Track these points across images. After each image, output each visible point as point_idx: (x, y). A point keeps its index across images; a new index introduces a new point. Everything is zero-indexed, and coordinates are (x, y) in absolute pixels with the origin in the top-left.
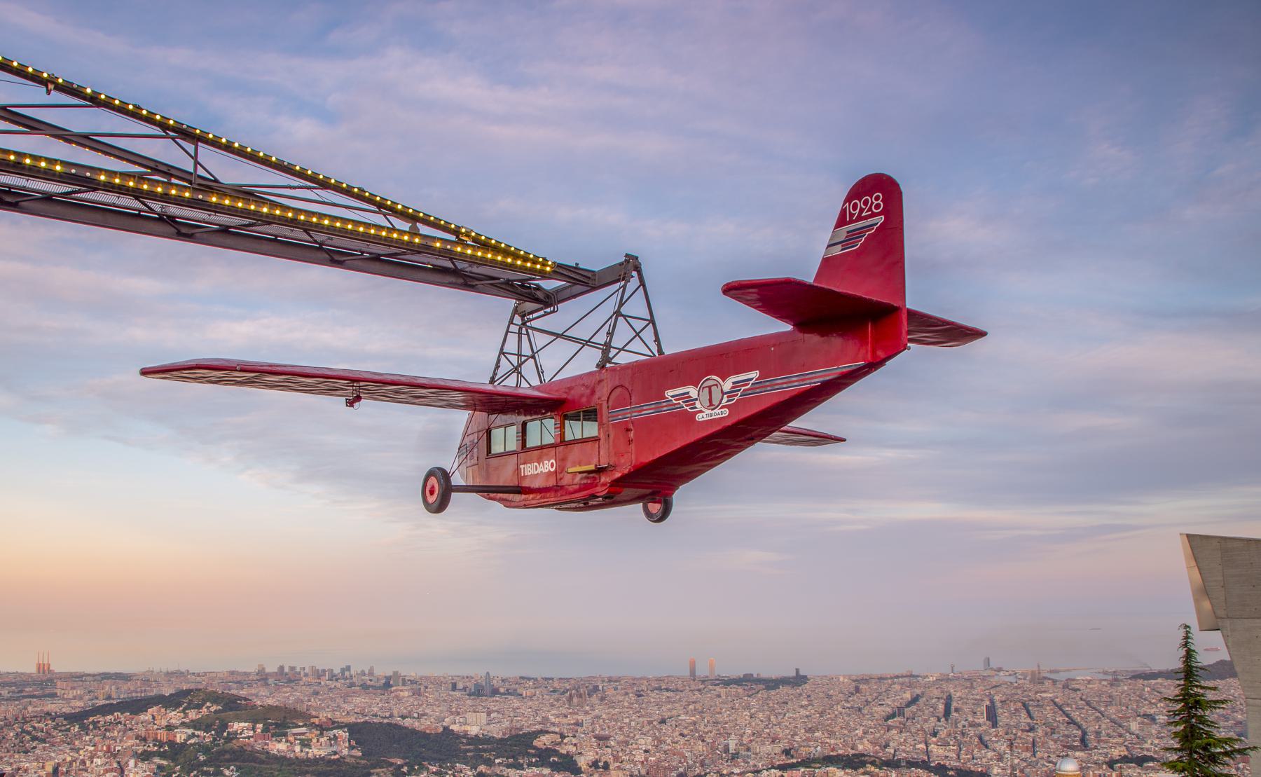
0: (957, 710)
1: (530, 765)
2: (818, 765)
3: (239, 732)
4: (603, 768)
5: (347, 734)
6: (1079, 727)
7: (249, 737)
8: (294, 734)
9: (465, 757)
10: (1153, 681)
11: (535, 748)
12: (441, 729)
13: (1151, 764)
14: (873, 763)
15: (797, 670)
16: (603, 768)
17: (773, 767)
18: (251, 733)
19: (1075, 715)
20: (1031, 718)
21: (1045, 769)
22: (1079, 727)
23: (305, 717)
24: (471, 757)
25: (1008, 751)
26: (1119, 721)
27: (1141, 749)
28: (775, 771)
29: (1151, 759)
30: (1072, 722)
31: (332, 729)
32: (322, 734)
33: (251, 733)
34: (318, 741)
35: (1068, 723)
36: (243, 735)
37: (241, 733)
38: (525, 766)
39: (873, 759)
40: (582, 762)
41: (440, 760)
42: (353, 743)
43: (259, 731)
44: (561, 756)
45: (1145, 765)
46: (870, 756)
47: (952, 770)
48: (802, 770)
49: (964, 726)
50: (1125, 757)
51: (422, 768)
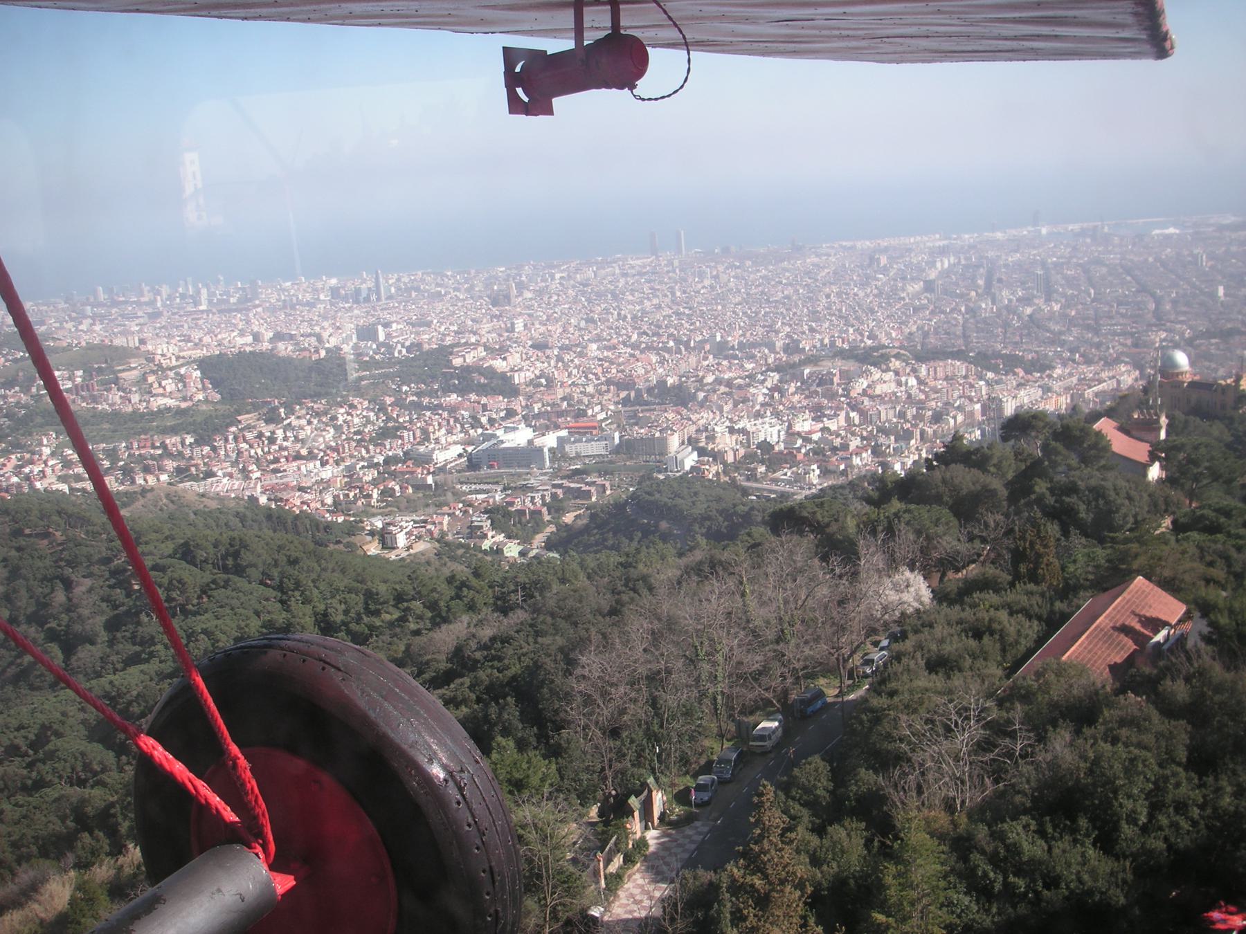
12: (323, 353)
22: (1153, 295)
43: (79, 380)
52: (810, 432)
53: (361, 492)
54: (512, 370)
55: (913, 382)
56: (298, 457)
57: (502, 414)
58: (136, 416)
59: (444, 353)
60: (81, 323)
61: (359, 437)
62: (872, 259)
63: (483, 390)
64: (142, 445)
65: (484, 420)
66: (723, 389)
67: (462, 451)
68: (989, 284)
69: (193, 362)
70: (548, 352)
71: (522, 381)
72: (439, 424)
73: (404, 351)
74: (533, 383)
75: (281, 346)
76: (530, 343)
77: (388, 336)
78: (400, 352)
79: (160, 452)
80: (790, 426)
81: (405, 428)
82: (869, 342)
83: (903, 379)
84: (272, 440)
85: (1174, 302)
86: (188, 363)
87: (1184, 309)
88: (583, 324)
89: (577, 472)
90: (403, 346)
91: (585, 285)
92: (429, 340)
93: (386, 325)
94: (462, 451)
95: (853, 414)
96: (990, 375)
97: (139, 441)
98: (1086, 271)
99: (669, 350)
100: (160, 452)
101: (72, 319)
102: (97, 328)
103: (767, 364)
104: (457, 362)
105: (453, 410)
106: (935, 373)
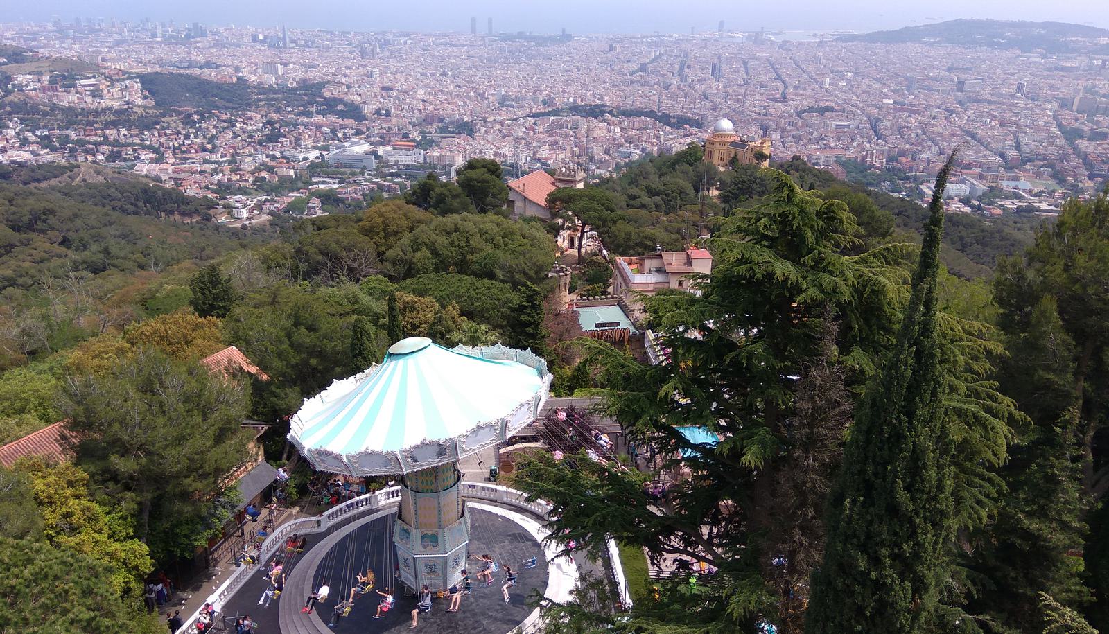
0: (689, 67)
1: (318, 113)
2: (566, 114)
3: (24, 84)
4: (385, 115)
5: (139, 85)
6: (784, 82)
7: (35, 90)
8: (83, 86)
9: (257, 106)
10: (850, 44)
11: (323, 97)
12: (235, 80)
13: (830, 113)
14: (611, 113)
15: (564, 31)
16: (385, 115)
17: (529, 116)
18: (38, 86)
19: (782, 71)
20: (747, 74)
22: (784, 82)
23: (95, 69)
24: (263, 106)
25: (723, 102)
26: (816, 77)
27: (827, 100)
29: (832, 109)
30: (779, 78)
31: (124, 80)
32: (112, 85)
33: (38, 86)
34: (109, 91)
35: (775, 79)
36: (29, 88)
37: (26, 86)
38: (315, 114)
39: (611, 109)
40: (367, 110)
41: (233, 108)
42: (146, 93)
44: (346, 104)
46: (609, 106)
47: (674, 118)
48: (552, 118)
49: (693, 81)
50: (812, 107)
51: (212, 115)
52: (547, 158)
53: (241, 177)
54: (364, 103)
55: (618, 130)
56: (204, 150)
57: (353, 132)
58: (85, 112)
59: (322, 85)
60: (63, 42)
62: (611, 46)
63: (342, 115)
64: (87, 133)
65: (340, 135)
66: (498, 126)
67: (318, 155)
68: (682, 69)
69: (137, 77)
70: (391, 93)
71: (370, 111)
72: (309, 136)
73: (295, 83)
74: (378, 112)
75: (206, 70)
76: (381, 85)
77: (286, 72)
78: (292, 84)
79: (102, 139)
80: (535, 153)
81: (285, 136)
82: (598, 102)
83: (612, 127)
84: (187, 137)
85: (797, 87)
86: (130, 78)
87: (802, 92)
88: (418, 76)
89: (392, 175)
90: (294, 80)
91: (425, 50)
92: (314, 76)
93: (286, 65)
94: (318, 155)
95: (575, 149)
97: (85, 130)
98: (745, 64)
99: (469, 98)
100: (102, 139)
101: (57, 38)
102: (76, 47)
103: (531, 112)
104: (327, 94)
105: (319, 127)
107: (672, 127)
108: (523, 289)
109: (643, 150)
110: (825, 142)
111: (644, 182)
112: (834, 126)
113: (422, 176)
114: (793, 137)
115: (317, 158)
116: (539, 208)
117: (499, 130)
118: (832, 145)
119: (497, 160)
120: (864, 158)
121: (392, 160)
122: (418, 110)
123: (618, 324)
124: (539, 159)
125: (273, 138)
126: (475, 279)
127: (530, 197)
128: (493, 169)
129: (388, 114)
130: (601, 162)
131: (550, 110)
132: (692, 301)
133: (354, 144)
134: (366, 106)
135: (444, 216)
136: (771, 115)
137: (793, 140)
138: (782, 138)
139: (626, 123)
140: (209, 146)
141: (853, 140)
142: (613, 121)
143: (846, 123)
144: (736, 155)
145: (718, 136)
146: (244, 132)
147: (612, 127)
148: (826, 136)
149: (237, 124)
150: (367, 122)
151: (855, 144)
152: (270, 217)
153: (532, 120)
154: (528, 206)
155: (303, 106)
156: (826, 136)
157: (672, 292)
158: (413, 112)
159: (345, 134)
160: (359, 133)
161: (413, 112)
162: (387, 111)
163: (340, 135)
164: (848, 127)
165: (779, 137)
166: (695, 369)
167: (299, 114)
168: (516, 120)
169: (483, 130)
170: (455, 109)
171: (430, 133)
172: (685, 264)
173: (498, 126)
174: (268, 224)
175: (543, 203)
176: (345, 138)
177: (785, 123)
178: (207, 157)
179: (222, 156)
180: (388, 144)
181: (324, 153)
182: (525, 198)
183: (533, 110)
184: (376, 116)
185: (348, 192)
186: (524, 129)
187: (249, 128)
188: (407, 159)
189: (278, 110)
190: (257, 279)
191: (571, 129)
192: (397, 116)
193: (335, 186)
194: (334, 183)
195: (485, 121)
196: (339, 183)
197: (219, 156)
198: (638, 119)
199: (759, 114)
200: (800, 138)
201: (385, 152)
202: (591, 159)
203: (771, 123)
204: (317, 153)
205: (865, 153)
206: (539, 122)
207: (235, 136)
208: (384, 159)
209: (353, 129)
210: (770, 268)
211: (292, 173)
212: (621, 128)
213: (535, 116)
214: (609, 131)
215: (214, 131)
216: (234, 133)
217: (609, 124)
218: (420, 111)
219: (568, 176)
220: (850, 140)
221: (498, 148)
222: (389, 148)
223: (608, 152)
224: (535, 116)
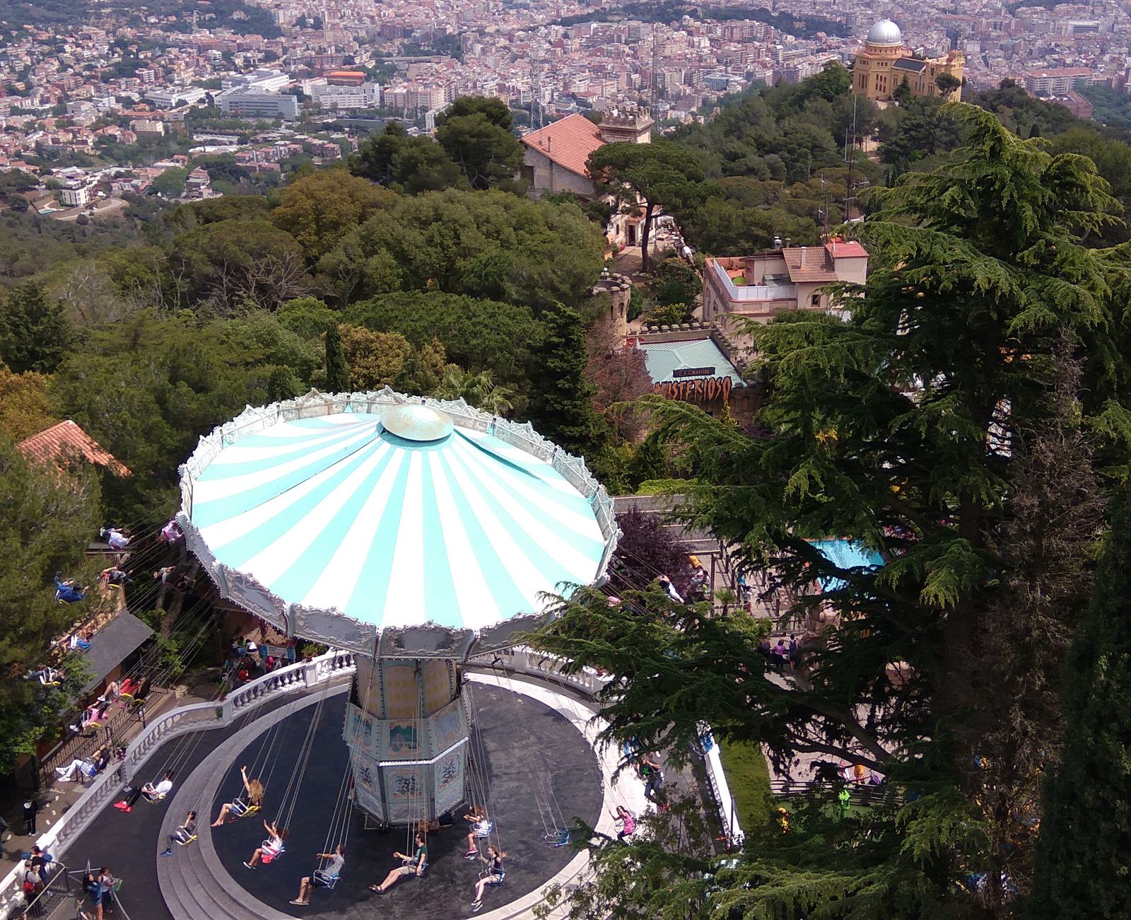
1: (202, 25)
2: (617, 18)
4: (313, 27)
9: (99, 16)
14: (693, 14)
16: (313, 27)
17: (555, 23)
21: (926, 16)
24: (109, 16)
28: (557, 28)
38: (195, 28)
40: (282, 18)
41: (59, 21)
45: (1058, 7)
47: (800, 20)
48: (594, 25)
51: (24, 33)
52: (588, 94)
53: (75, 137)
54: (277, 6)
55: (705, 43)
56: (13, 92)
57: (260, 56)
61: (88, 73)
65: (239, 62)
66: (503, 42)
67: (203, 96)
71: (287, 20)
72: (187, 64)
74: (301, 22)
80: (566, 86)
81: (146, 66)
83: (696, 39)
89: (327, 127)
94: (203, 96)
95: (634, 76)
96: (791, 38)
103: (558, 15)
105: (203, 49)
106: (732, 34)
107: (797, 36)
108: (551, 315)
109: (749, 75)
110: (1056, 56)
111: (750, 131)
112: (1070, 29)
113: (377, 128)
114: (1001, 48)
115: (201, 101)
116: (575, 179)
117: (505, 48)
118: (1069, 61)
119: (503, 99)
120: (1122, 81)
121: (326, 102)
122: (367, 16)
123: (712, 371)
124: (573, 96)
125: (127, 70)
126: (470, 301)
127: (561, 160)
128: (496, 113)
129: (318, 25)
130: (678, 97)
131: (591, 11)
132: (835, 329)
133: (262, 76)
134: (281, 12)
135: (415, 195)
136: (965, 13)
137: (1001, 53)
138: (983, 50)
139: (719, 32)
140: (20, 86)
141: (1103, 52)
142: (698, 29)
143: (1091, 23)
144: (905, 81)
145: (875, 49)
146: (78, 61)
147: (696, 39)
148: (1057, 46)
149: (67, 47)
150: (283, 39)
151: (1107, 58)
152: (125, 203)
153: (561, 29)
154: (556, 175)
155: (176, 14)
156: (1057, 46)
157: (802, 315)
158: (360, 20)
159: (246, 60)
160: (269, 57)
161: (360, 20)
162: (316, 19)
163: (239, 62)
164: (1095, 28)
165: (977, 49)
166: (842, 445)
167: (170, 28)
168: (533, 29)
169: (478, 47)
170: (431, 14)
171: (389, 55)
172: (822, 267)
173: (503, 42)
174: (121, 214)
175: (581, 169)
176: (246, 67)
177: (988, 25)
178: (17, 104)
179: (42, 102)
180: (320, 75)
181: (213, 94)
182: (552, 162)
183: (563, 13)
184: (298, 28)
185: (255, 157)
186: (547, 46)
187: (86, 53)
188: (352, 99)
189: (134, 22)
190: (105, 307)
191: (627, 43)
192: (334, 26)
193: (233, 149)
194: (231, 143)
195: (482, 33)
196: (240, 142)
197: (37, 101)
198: (739, 23)
199: (944, 11)
200: (1014, 49)
201: (315, 88)
202: (662, 94)
203: (963, 25)
204: (201, 93)
205: (1123, 73)
206: (572, 33)
207: (64, 67)
208: (314, 101)
209: (260, 51)
210: (965, 272)
211: (159, 127)
212: (711, 40)
213: (566, 22)
214: (691, 45)
215: (28, 60)
216: (61, 63)
217: (690, 33)
218: (372, 18)
219: (624, 122)
220: (1098, 51)
221: (504, 78)
222: (321, 82)
223: (688, 81)
224: (566, 22)
